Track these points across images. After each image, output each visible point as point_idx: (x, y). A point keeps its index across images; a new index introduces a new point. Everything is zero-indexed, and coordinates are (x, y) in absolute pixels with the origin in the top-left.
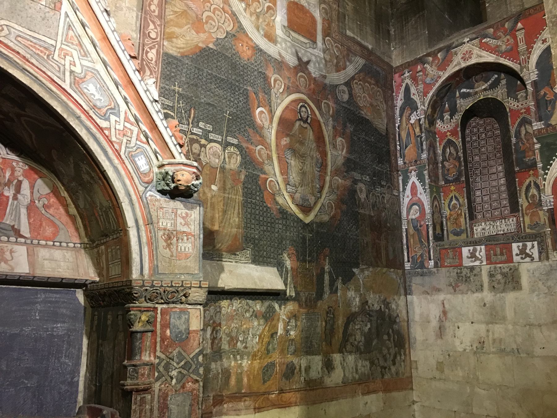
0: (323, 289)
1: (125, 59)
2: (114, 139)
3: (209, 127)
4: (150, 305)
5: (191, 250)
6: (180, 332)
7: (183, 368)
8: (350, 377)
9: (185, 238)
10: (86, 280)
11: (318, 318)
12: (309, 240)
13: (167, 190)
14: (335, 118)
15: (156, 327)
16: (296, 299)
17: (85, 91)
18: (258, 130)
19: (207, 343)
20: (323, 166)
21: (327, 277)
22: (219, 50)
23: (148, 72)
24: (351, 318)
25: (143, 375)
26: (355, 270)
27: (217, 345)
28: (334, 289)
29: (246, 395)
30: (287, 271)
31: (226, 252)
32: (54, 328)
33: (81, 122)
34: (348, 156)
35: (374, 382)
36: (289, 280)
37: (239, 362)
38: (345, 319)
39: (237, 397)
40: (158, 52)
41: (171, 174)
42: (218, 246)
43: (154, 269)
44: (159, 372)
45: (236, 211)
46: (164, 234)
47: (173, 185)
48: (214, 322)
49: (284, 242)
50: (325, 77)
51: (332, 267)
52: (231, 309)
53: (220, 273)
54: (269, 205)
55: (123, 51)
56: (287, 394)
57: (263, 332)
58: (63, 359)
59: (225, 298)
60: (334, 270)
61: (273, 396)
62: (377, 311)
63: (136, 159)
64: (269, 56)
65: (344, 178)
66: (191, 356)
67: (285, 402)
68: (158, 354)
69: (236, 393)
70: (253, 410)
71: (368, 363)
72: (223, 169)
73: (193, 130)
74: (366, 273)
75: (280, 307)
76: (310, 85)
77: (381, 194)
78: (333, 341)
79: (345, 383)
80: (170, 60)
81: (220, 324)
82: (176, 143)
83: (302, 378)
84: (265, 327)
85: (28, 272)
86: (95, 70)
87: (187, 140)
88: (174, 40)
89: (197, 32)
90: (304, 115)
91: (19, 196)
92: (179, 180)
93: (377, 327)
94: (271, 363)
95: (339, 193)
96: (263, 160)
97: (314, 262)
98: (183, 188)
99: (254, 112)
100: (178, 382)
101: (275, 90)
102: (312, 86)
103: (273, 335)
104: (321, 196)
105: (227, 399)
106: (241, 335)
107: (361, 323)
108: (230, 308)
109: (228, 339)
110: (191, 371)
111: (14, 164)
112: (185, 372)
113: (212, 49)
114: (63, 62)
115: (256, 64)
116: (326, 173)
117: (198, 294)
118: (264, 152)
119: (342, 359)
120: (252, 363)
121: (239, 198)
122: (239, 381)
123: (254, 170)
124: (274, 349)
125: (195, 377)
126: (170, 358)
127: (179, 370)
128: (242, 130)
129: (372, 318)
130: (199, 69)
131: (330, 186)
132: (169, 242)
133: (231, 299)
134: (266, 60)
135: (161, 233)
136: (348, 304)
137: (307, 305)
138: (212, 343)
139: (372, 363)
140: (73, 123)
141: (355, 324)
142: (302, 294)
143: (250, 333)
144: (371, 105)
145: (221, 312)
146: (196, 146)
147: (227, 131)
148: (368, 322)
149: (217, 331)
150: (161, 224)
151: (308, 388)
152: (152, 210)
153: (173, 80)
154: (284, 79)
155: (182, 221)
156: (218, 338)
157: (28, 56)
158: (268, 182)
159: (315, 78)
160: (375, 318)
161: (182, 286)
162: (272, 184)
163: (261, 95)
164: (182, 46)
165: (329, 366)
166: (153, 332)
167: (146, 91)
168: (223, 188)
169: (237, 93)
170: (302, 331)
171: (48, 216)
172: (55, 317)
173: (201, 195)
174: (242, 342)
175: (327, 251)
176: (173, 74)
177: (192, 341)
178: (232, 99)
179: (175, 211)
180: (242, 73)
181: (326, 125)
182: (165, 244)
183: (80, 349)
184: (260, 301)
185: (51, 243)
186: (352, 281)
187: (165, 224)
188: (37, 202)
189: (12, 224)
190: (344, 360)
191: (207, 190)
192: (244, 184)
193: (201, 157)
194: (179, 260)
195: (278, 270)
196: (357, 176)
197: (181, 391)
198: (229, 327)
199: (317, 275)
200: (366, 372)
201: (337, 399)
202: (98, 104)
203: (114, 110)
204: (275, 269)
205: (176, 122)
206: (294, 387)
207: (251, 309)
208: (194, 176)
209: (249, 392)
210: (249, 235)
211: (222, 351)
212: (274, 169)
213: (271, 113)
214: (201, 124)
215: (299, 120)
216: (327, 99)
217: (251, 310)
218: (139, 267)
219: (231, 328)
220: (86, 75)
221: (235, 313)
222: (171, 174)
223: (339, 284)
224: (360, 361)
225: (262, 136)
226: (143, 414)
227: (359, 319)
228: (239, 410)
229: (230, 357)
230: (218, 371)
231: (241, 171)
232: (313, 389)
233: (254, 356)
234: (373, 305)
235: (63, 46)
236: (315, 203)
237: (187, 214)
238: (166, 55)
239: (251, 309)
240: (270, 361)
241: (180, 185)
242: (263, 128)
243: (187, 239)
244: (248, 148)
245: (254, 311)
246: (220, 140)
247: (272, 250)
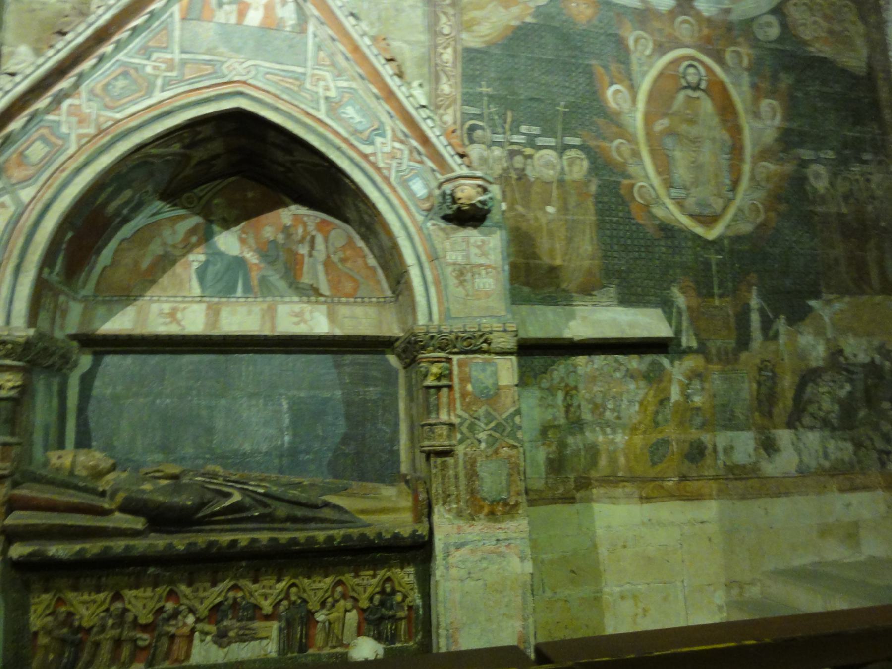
0: (749, 336)
1: (379, 64)
2: (381, 165)
3: (535, 130)
4: (442, 354)
5: (492, 287)
6: (487, 387)
7: (495, 431)
8: (813, 464)
9: (483, 272)
10: (391, 337)
11: (743, 377)
12: (717, 264)
13: (450, 215)
14: (754, 69)
15: (451, 379)
16: (702, 350)
17: (344, 116)
18: (614, 119)
19: (559, 411)
20: (736, 150)
21: (755, 319)
22: (542, 22)
23: (444, 79)
24: (808, 377)
25: (440, 435)
26: (812, 303)
27: (575, 412)
28: (771, 333)
29: (624, 480)
30: (680, 313)
31: (576, 292)
32: (365, 392)
33: (343, 153)
34: (787, 125)
35: (864, 474)
36: (685, 324)
37: (611, 437)
38: (797, 379)
39: (612, 480)
40: (455, 51)
41: (449, 192)
42: (564, 286)
43: (446, 314)
44: (462, 433)
45: (588, 236)
46: (454, 270)
47: (455, 206)
48: (567, 385)
49: (671, 272)
50: (728, 11)
51: (764, 301)
53: (568, 320)
54: (641, 222)
55: (376, 56)
56: (694, 482)
57: (645, 398)
58: (379, 426)
60: (768, 305)
61: (671, 483)
62: (864, 365)
63: (411, 184)
64: (624, 7)
65: (780, 161)
66: (505, 416)
68: (459, 412)
69: (609, 476)
71: (849, 446)
72: (561, 182)
73: (512, 139)
74: (838, 306)
75: (672, 362)
76: (700, 30)
77: (862, 175)
78: (776, 411)
79: (803, 472)
80: (472, 55)
81: (576, 388)
82: (453, 153)
83: (720, 463)
85: (327, 331)
86: (351, 88)
87: (505, 153)
88: (475, 28)
89: (507, 7)
90: (692, 79)
91: (315, 253)
92: (460, 199)
93: (867, 390)
94: (663, 439)
95: (770, 186)
96: (625, 159)
97: (728, 296)
98: (467, 208)
99: (604, 93)
100: (490, 445)
101: (637, 54)
102: (706, 31)
103: (663, 402)
104: (735, 195)
105: (595, 484)
106: (610, 402)
107: (831, 384)
108: (590, 366)
109: (590, 406)
110: (505, 433)
111: (305, 219)
112: (497, 435)
113: (530, 23)
114: (314, 89)
115: (601, 25)
116: (741, 160)
117: (502, 340)
118: (626, 149)
119: (795, 438)
120: (631, 439)
121: (591, 217)
122: (613, 461)
123: (610, 176)
125: (512, 442)
126: (476, 418)
127: (489, 432)
128: (587, 123)
129: (854, 376)
130: (513, 56)
131: (753, 178)
132: (462, 278)
134: (619, 15)
135: (450, 269)
136: (801, 356)
137: (720, 360)
138: (567, 411)
139: (858, 445)
140: (333, 156)
141: (817, 384)
142: (710, 344)
144: (831, 32)
146: (518, 161)
147: (564, 129)
148: (847, 381)
149: (572, 397)
150: (448, 257)
152: (436, 242)
153: (478, 80)
154: (651, 34)
155: (477, 251)
157: (278, 93)
158: (636, 189)
159: (709, 20)
160: (862, 376)
161: (479, 330)
162: (644, 190)
163: (613, 67)
164: (487, 32)
165: (769, 446)
166: (450, 387)
167: (407, 97)
168: (564, 208)
169: (574, 74)
171: (347, 270)
172: (365, 380)
173: (532, 222)
174: (613, 411)
175: (753, 277)
176: (478, 73)
177: (503, 399)
178: (567, 84)
179: (466, 240)
180: (579, 44)
181: (738, 84)
182: (456, 282)
183: (397, 415)
185: (352, 300)
186: (807, 321)
187: (454, 257)
188: (332, 256)
189: (311, 283)
190: (799, 439)
191: (539, 214)
192: (596, 198)
193: (529, 172)
194: (479, 299)
195: (664, 312)
196: (806, 153)
197: (494, 457)
199: (737, 315)
200: (847, 459)
201: (787, 494)
202: (359, 128)
203: (379, 131)
204: (658, 312)
205: (488, 133)
206: (706, 474)
207: (623, 368)
208: (480, 190)
210: (610, 267)
212: (644, 169)
213: (633, 89)
214: (524, 129)
215: (685, 88)
216: (735, 44)
217: (623, 368)
218: (426, 311)
220: (343, 97)
221: (598, 373)
222: (449, 192)
223: (781, 325)
224: (832, 442)
225: (620, 126)
226: (446, 480)
227: (826, 377)
228: (615, 497)
231: (590, 181)
232: (741, 479)
233: (634, 429)
234: (855, 356)
235: (316, 72)
236: (725, 208)
237: (483, 241)
238: (468, 50)
239: (623, 368)
240: (660, 436)
241: (462, 204)
242: (619, 114)
243: (487, 273)
244: (598, 147)
245: (628, 370)
246: (553, 144)
247: (651, 284)
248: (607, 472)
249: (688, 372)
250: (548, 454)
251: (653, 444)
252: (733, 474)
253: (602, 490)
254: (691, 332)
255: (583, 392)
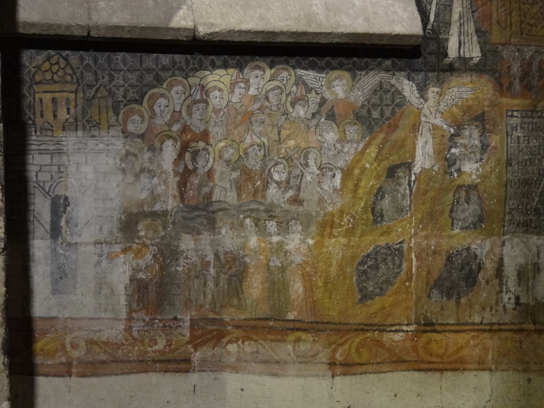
48: (185, 129)
52: (243, 96)
59: (218, 63)
61: (398, 337)
67: (442, 356)
70: (326, 367)
81: (205, 135)
83: (508, 299)
84: (367, 146)
105: (238, 333)
106: (280, 167)
108: (237, 91)
124: (400, 210)
133: (240, 67)
138: (182, 185)
143: (311, 162)
145: (206, 102)
149: (195, 154)
151: (531, 327)
156: (201, 171)
170: (509, 163)
174: (285, 185)
184: (346, 74)
198: (235, 143)
209: (313, 319)
211: (216, 206)
219: (243, 146)
221: (257, 106)
229: (242, 225)
230: (203, 258)
240: (383, 241)
245: (323, 102)
248: (264, 310)
249: (455, 109)
250: (136, 270)
251: (368, 256)
252: (535, 324)
253: (249, 347)
254: (471, 28)
255: (222, 144)
